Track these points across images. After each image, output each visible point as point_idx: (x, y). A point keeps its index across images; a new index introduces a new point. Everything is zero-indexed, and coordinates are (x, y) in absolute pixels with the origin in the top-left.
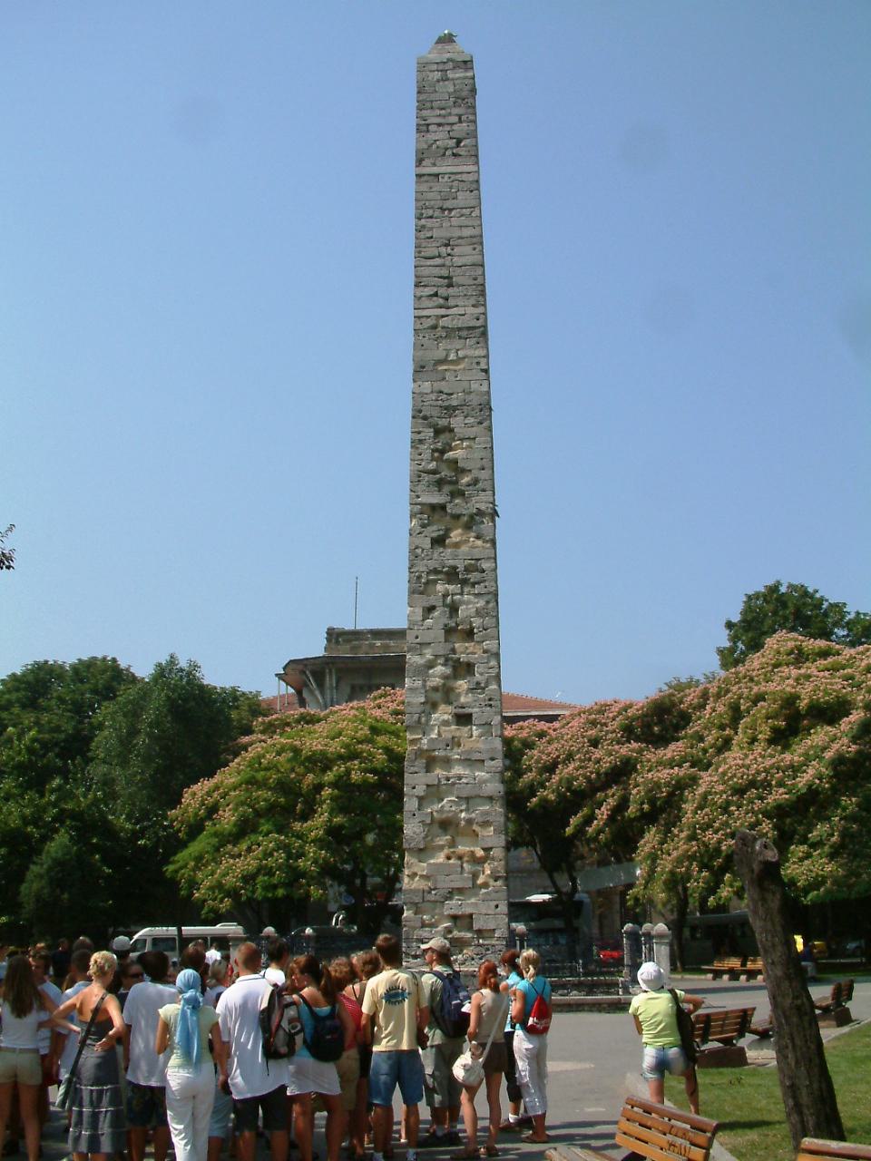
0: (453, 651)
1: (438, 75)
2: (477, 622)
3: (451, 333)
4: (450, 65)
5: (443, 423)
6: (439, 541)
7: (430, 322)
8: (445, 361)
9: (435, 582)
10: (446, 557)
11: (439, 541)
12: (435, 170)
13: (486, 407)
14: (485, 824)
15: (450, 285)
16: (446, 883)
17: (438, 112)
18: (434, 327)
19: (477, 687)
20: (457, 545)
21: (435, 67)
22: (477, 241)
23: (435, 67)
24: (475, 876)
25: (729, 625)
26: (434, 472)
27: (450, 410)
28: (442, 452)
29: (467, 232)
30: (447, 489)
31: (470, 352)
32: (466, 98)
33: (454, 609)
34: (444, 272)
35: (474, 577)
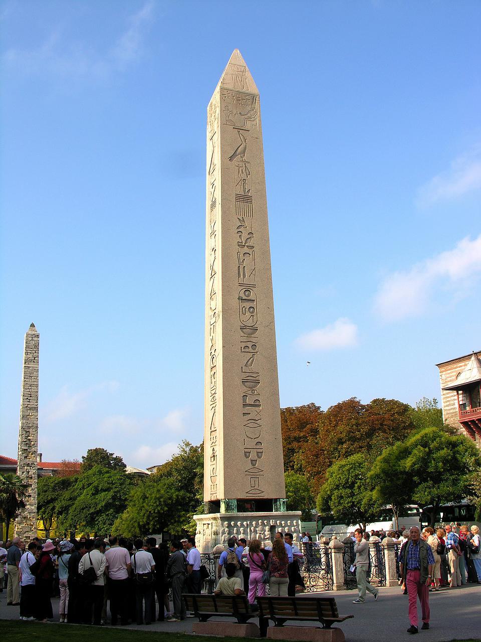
0: (28, 482)
1: (31, 339)
2: (33, 476)
3: (30, 409)
4: (34, 336)
5: (28, 430)
6: (26, 457)
7: (26, 405)
8: (29, 415)
9: (25, 466)
10: (27, 461)
11: (26, 457)
12: (29, 366)
13: (37, 427)
14: (33, 518)
15: (31, 397)
16: (25, 530)
17: (30, 349)
18: (27, 407)
19: (33, 489)
20: (29, 458)
21: (30, 336)
22: (37, 386)
23: (30, 336)
24: (31, 528)
25: (83, 457)
26: (25, 442)
27: (29, 427)
28: (27, 437)
29: (35, 383)
30: (28, 445)
31: (34, 414)
32: (37, 346)
33: (28, 472)
34: (30, 393)
35: (33, 466)
